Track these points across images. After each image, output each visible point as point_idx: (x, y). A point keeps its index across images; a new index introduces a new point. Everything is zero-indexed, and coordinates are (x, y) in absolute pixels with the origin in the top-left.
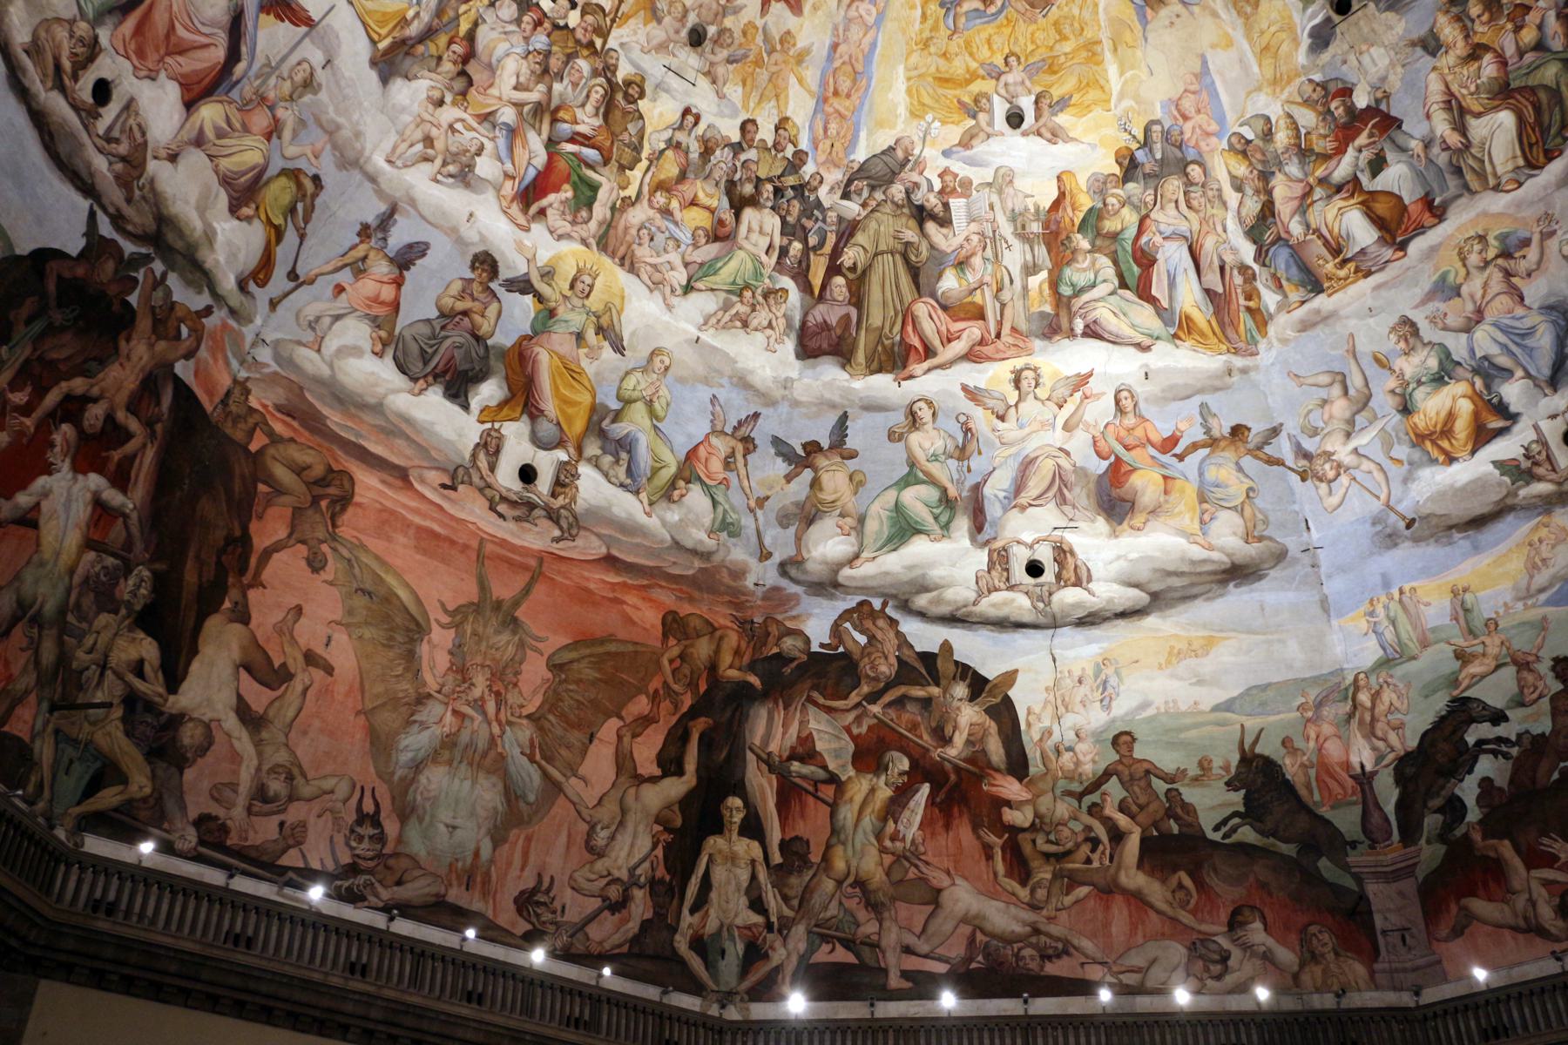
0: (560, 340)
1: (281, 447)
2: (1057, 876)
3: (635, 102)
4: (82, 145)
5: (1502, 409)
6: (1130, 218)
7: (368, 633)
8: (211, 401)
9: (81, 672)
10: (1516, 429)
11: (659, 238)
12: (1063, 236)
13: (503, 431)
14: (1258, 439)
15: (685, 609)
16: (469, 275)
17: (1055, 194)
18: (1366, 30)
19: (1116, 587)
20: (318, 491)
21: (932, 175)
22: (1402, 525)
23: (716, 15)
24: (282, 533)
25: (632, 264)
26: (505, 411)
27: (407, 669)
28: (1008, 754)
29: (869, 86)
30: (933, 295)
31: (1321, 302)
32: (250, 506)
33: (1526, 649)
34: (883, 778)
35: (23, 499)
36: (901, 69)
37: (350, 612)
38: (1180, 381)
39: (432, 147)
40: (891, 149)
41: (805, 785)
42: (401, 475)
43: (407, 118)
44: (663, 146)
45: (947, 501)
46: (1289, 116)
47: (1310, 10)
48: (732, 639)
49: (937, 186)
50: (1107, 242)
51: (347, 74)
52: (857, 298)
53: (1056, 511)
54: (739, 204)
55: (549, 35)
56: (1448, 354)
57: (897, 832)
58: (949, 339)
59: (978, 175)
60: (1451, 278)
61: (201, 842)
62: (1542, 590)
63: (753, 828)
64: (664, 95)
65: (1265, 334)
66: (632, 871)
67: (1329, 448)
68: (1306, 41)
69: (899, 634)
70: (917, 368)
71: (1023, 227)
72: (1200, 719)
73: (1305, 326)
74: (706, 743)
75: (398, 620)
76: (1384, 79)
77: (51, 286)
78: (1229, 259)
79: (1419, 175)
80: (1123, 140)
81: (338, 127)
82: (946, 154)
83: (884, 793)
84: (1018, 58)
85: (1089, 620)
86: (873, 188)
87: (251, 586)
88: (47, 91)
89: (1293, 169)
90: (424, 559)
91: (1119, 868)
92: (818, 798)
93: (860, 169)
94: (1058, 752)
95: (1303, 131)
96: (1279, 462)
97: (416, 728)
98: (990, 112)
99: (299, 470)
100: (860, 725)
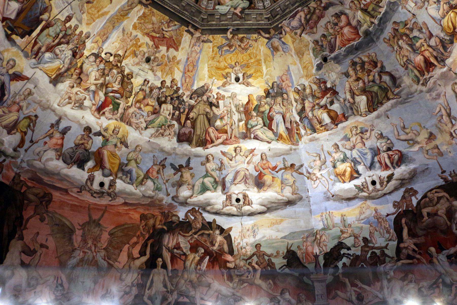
0: (110, 147)
1: (31, 190)
2: (239, 280)
3: (130, 79)
5: (357, 172)
6: (267, 107)
7: (58, 236)
10: (360, 178)
11: (138, 115)
13: (94, 174)
14: (297, 168)
15: (146, 212)
16: (83, 133)
17: (247, 100)
18: (331, 67)
19: (258, 206)
21: (214, 94)
22: (331, 196)
24: (32, 213)
25: (130, 123)
26: (95, 169)
27: (69, 243)
28: (229, 249)
30: (214, 126)
31: (315, 135)
33: (357, 233)
34: (197, 254)
36: (206, 65)
37: (53, 231)
38: (278, 152)
39: (71, 99)
40: (203, 86)
41: (178, 255)
42: (66, 191)
43: (63, 92)
44: (138, 90)
45: (216, 182)
46: (310, 86)
48: (159, 218)
49: (216, 97)
50: (261, 114)
51: (42, 88)
52: (194, 126)
53: (244, 185)
54: (160, 103)
55: (104, 64)
56: (346, 155)
57: (200, 268)
58: (218, 138)
59: (227, 94)
60: (348, 136)
62: (362, 220)
63: (164, 266)
64: (139, 77)
66: (132, 283)
67: (315, 172)
68: (315, 67)
69: (202, 217)
70: (209, 146)
71: (239, 109)
72: (277, 241)
73: (311, 140)
74: (152, 246)
76: (335, 81)
78: (293, 119)
80: (266, 86)
81: (41, 101)
82: (218, 88)
83: (198, 258)
84: (239, 63)
85: (251, 214)
86: (198, 97)
89: (310, 99)
91: (255, 279)
92: (181, 259)
94: (242, 249)
96: (302, 174)
97: (72, 258)
98: (231, 77)
99: (36, 195)
100: (192, 240)
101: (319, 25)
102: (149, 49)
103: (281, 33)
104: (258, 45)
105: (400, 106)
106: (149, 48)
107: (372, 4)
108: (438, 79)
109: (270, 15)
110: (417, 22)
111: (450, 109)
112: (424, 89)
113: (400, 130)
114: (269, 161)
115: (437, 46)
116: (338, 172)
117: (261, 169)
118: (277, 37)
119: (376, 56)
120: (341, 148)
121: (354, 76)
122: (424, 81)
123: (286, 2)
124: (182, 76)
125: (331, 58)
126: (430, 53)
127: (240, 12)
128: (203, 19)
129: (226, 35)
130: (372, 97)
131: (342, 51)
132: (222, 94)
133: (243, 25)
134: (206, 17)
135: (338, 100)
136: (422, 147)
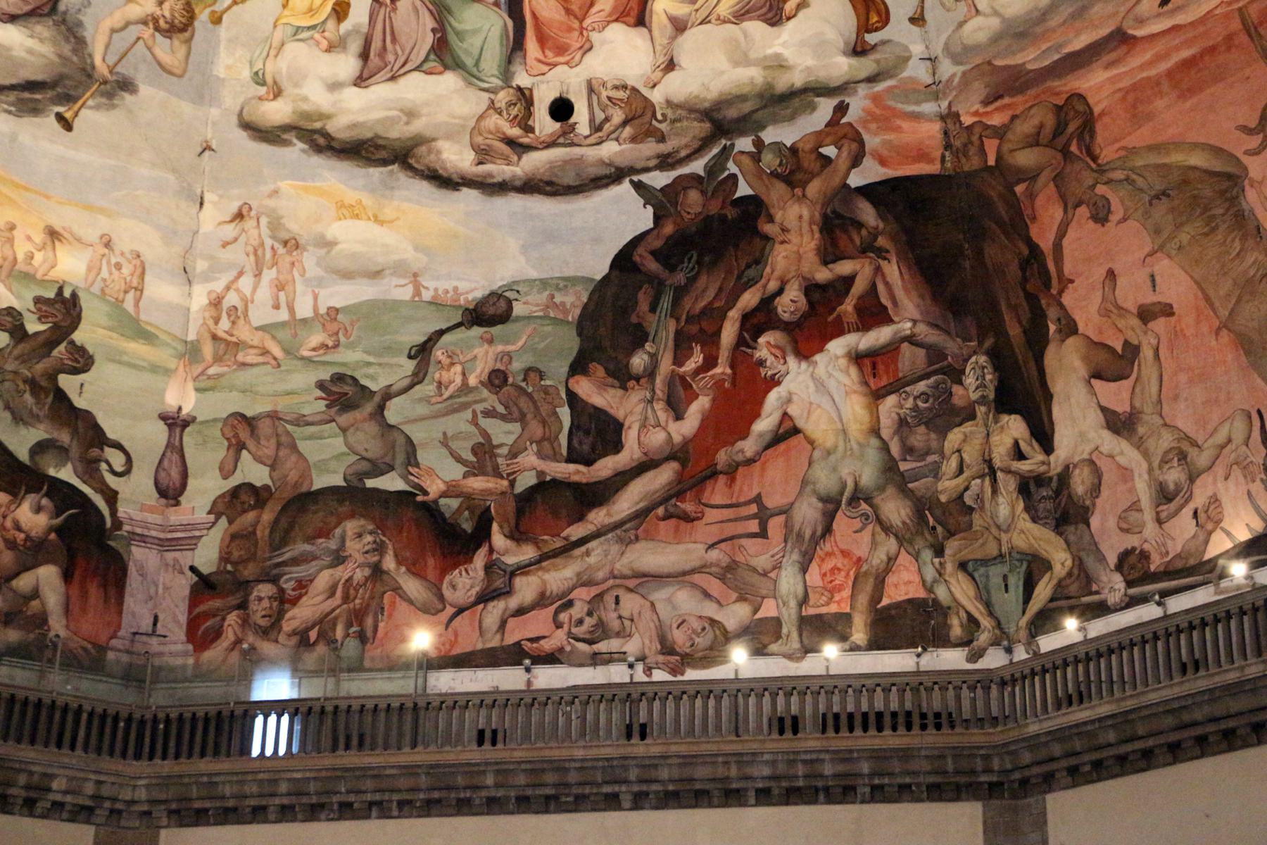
1: (1010, 136)
4: (581, 159)
7: (1184, 237)
8: (931, 161)
9: (961, 496)
20: (1062, 140)
24: (1058, 213)
27: (1244, 238)
32: (1021, 214)
35: (764, 425)
37: (1157, 231)
42: (1121, 39)
61: (1130, 584)
75: (1207, 192)
77: (652, 266)
87: (1061, 292)
88: (518, 165)
90: (1194, 100)
99: (1034, 141)
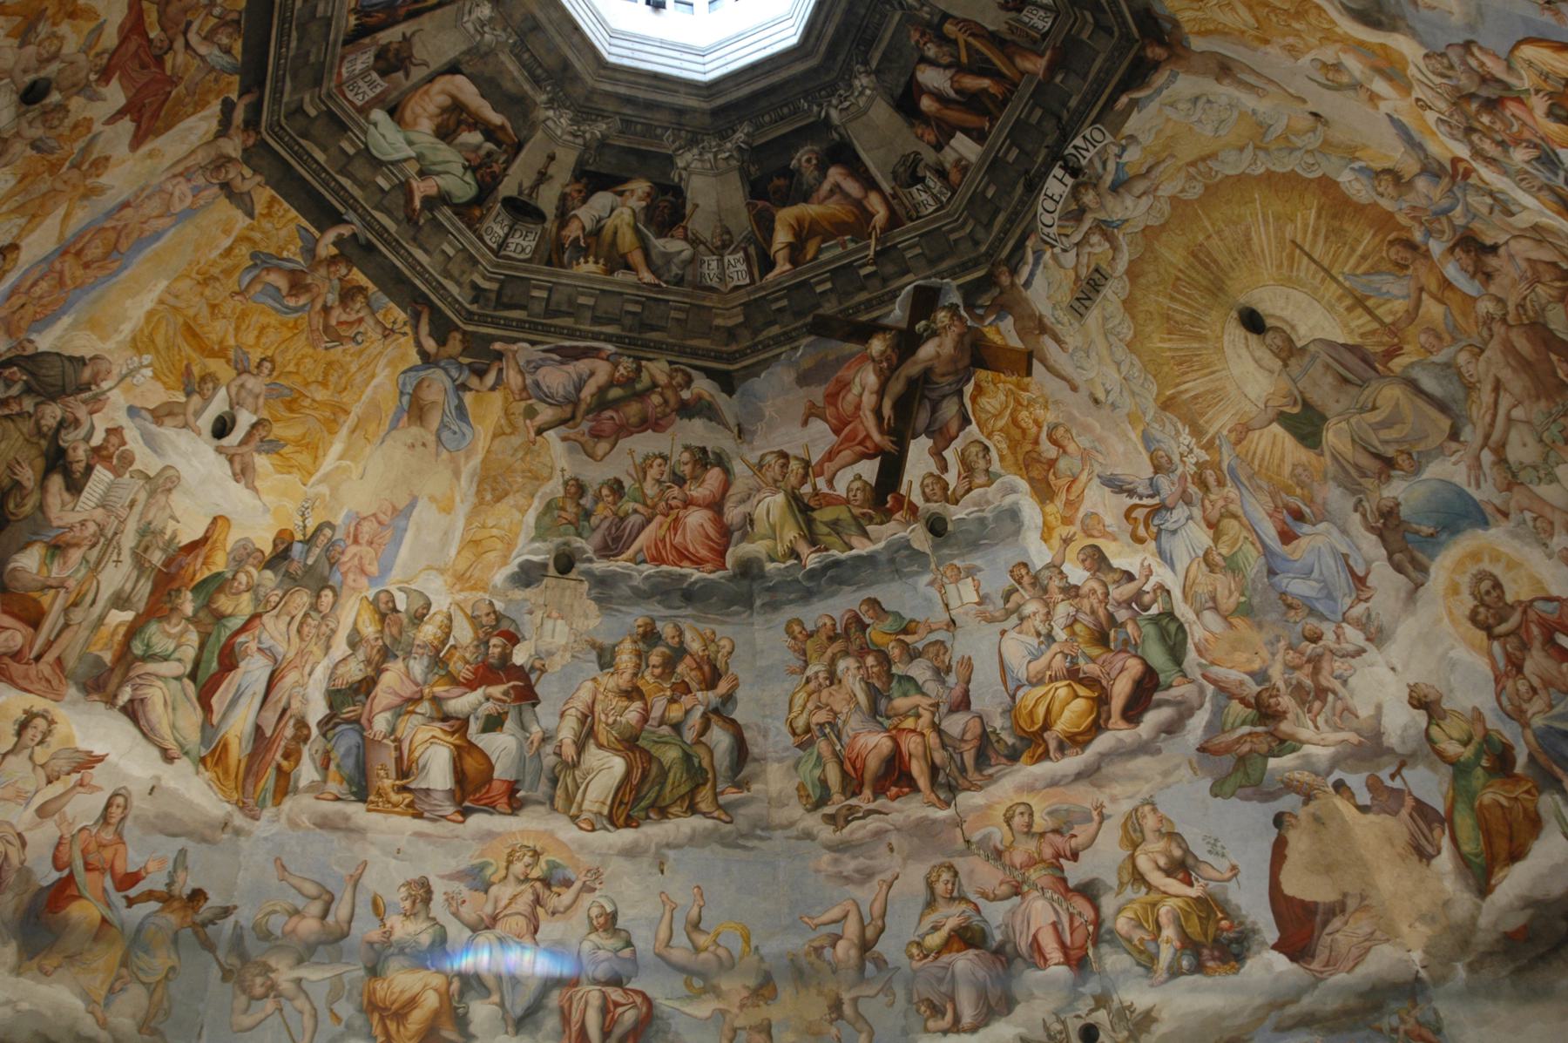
6: (245, 605)
12: (175, 586)
17: (198, 534)
18: (567, 601)
23: (74, 85)
29: (115, 274)
31: (356, 810)
36: (163, 284)
40: (82, 361)
46: (450, 618)
47: (537, 545)
49: (97, 440)
59: (145, 460)
60: (489, 871)
65: (277, 803)
67: (273, 962)
68: (513, 567)
71: (146, 549)
73: (324, 823)
76: (550, 654)
78: (295, 705)
79: (522, 759)
80: (294, 523)
82: (132, 411)
84: (273, 370)
86: (28, 390)
89: (418, 667)
93: (29, 357)
95: (452, 642)
98: (207, 401)
101: (625, 443)
102: (82, 57)
103: (481, 373)
104: (381, 353)
105: (717, 848)
106: (85, 50)
107: (843, 508)
108: (898, 830)
109: (494, 286)
110: (948, 645)
111: (882, 930)
112: (826, 833)
113: (679, 927)
114: (127, 836)
115: (962, 740)
116: (380, 994)
117: (79, 864)
118: (455, 374)
119: (730, 653)
120: (438, 907)
121: (627, 676)
122: (844, 812)
123: (582, 294)
124: (45, 259)
125: (589, 574)
126: (927, 752)
127: (429, 202)
128: (300, 110)
129: (317, 234)
130: (644, 776)
131: (640, 572)
132: (131, 445)
133: (395, 246)
134: (313, 112)
135: (523, 727)
136: (723, 1012)
